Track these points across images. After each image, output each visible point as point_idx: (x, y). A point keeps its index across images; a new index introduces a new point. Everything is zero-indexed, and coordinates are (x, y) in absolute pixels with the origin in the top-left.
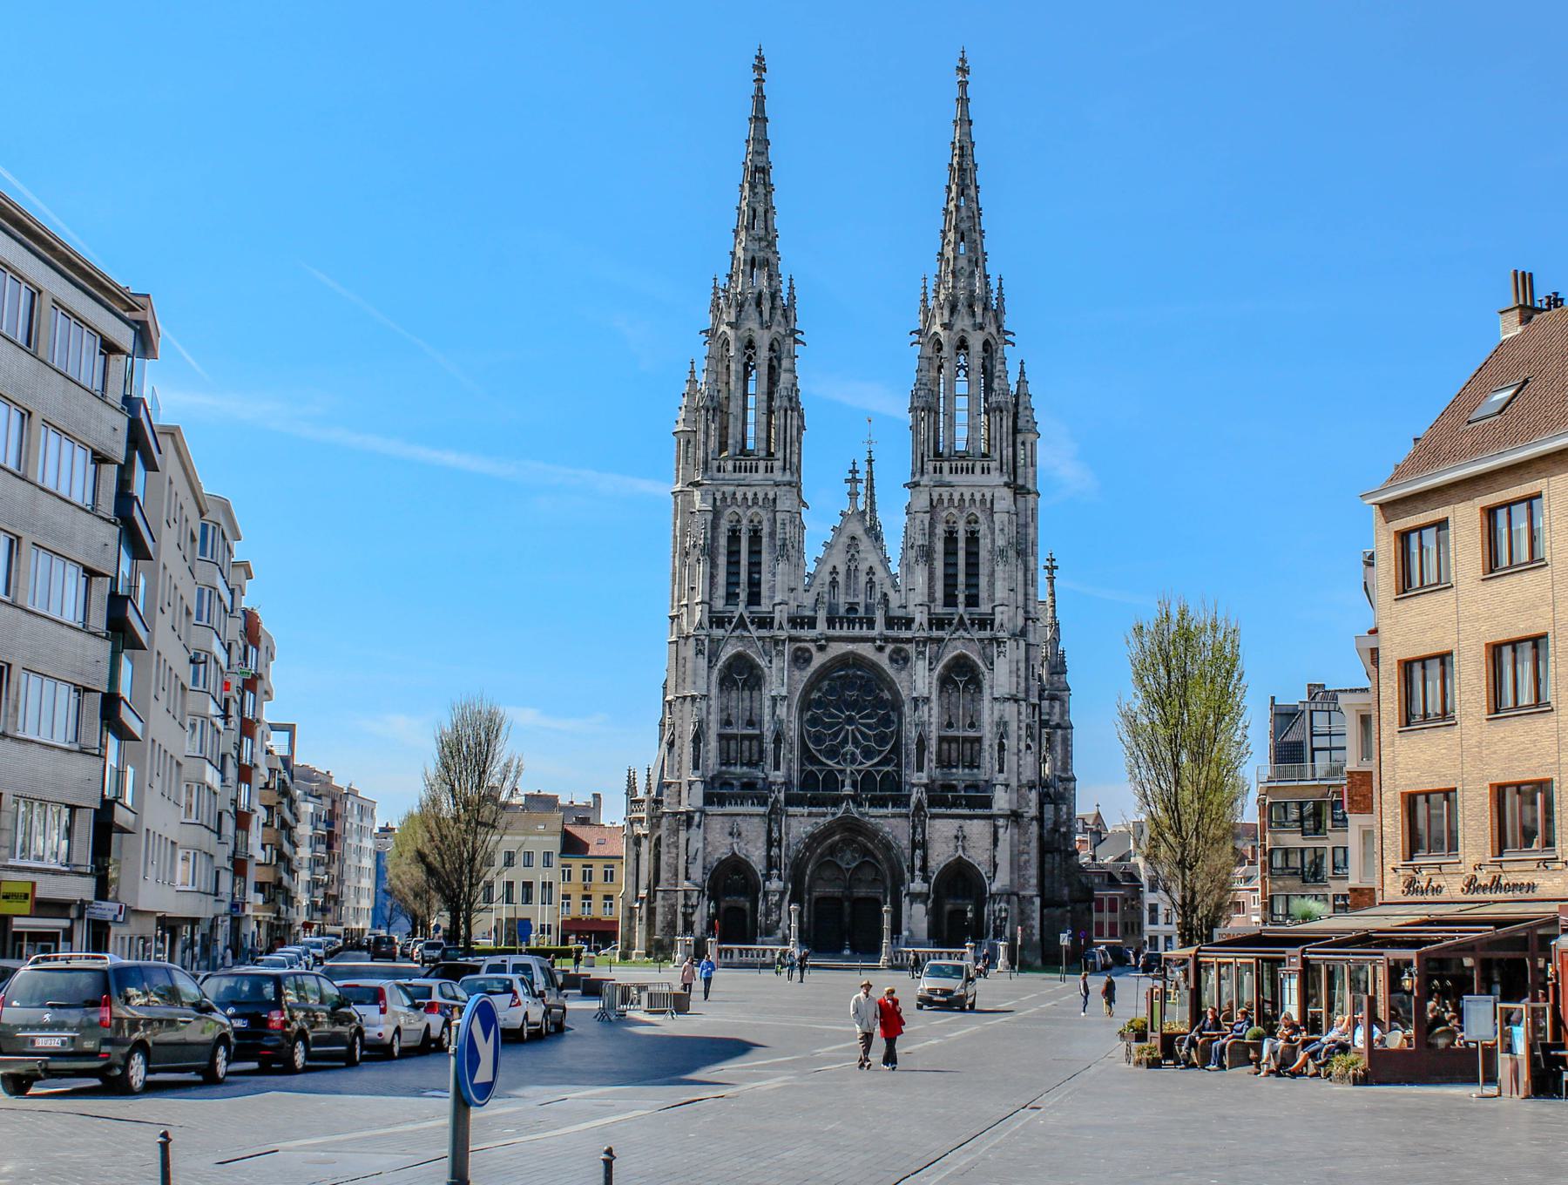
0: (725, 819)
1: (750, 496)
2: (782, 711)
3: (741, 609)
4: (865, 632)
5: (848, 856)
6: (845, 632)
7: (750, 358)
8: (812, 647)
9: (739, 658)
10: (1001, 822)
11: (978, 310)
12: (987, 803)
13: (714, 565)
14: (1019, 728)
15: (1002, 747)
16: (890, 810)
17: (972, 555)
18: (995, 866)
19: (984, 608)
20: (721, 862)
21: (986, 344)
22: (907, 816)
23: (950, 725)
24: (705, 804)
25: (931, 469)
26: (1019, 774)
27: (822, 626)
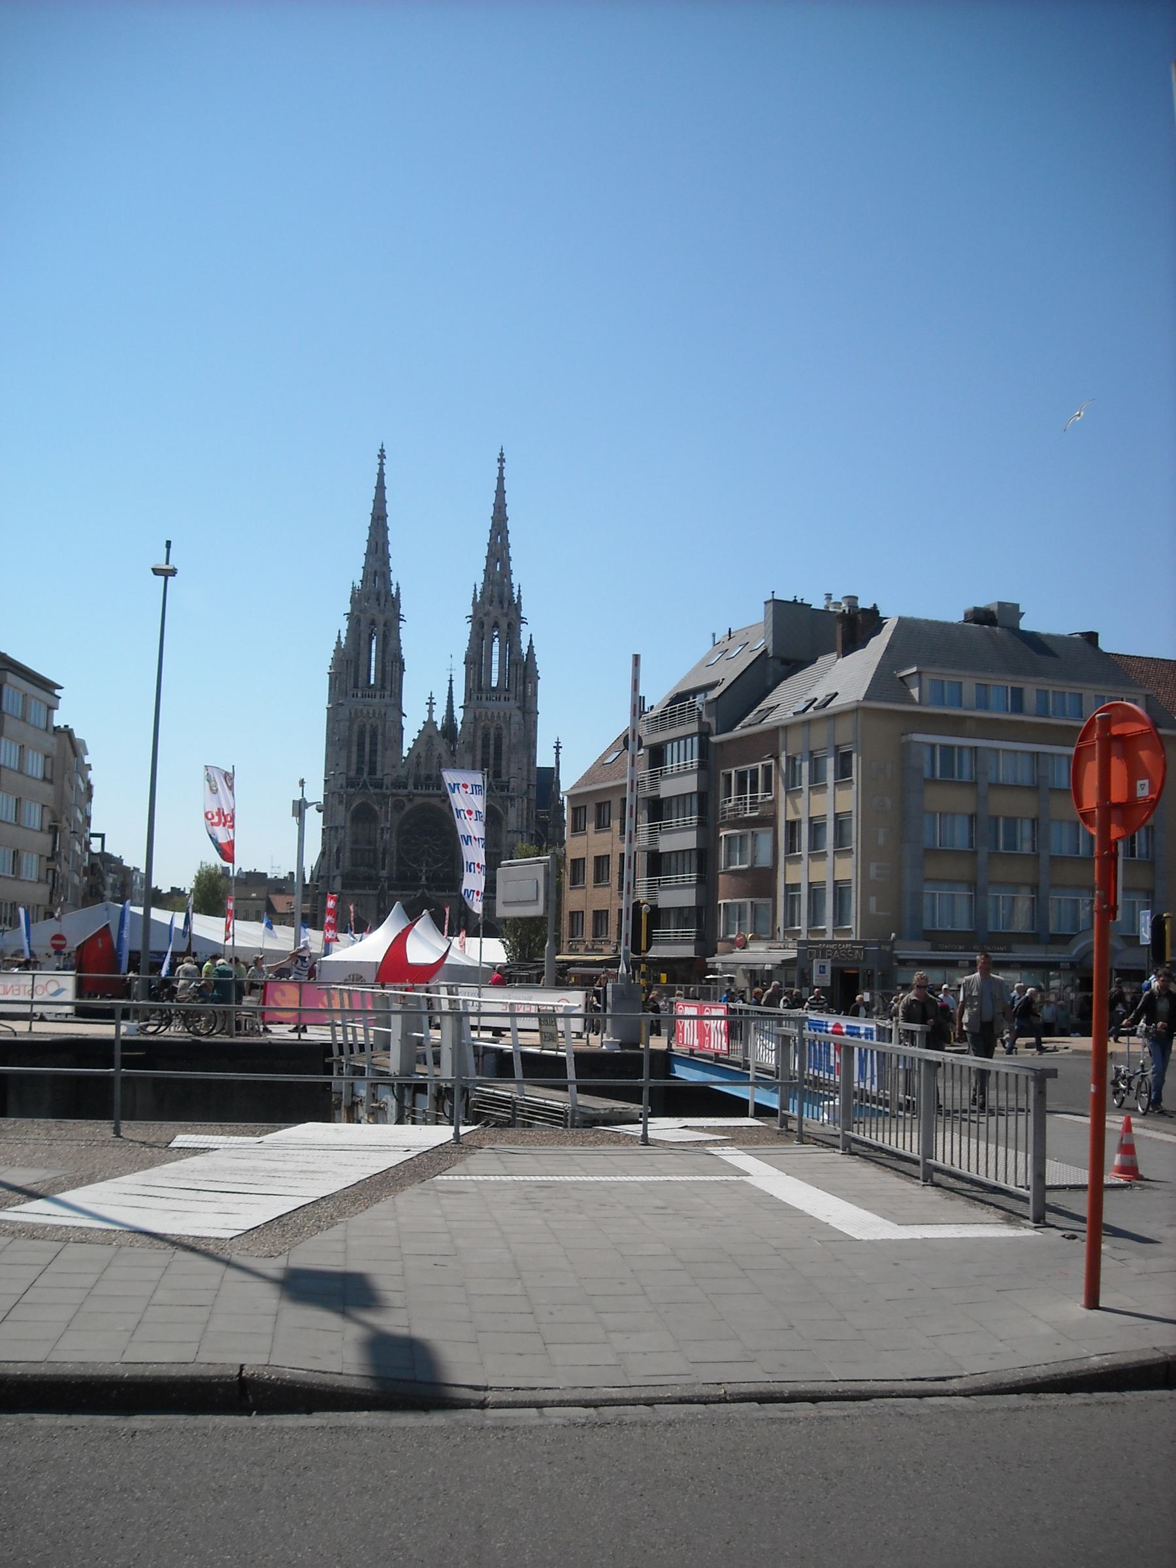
2: (386, 836)
4: (436, 792)
6: (423, 792)
8: (405, 799)
9: (363, 804)
11: (506, 605)
13: (349, 752)
16: (447, 893)
17: (498, 748)
21: (509, 625)
27: (411, 787)
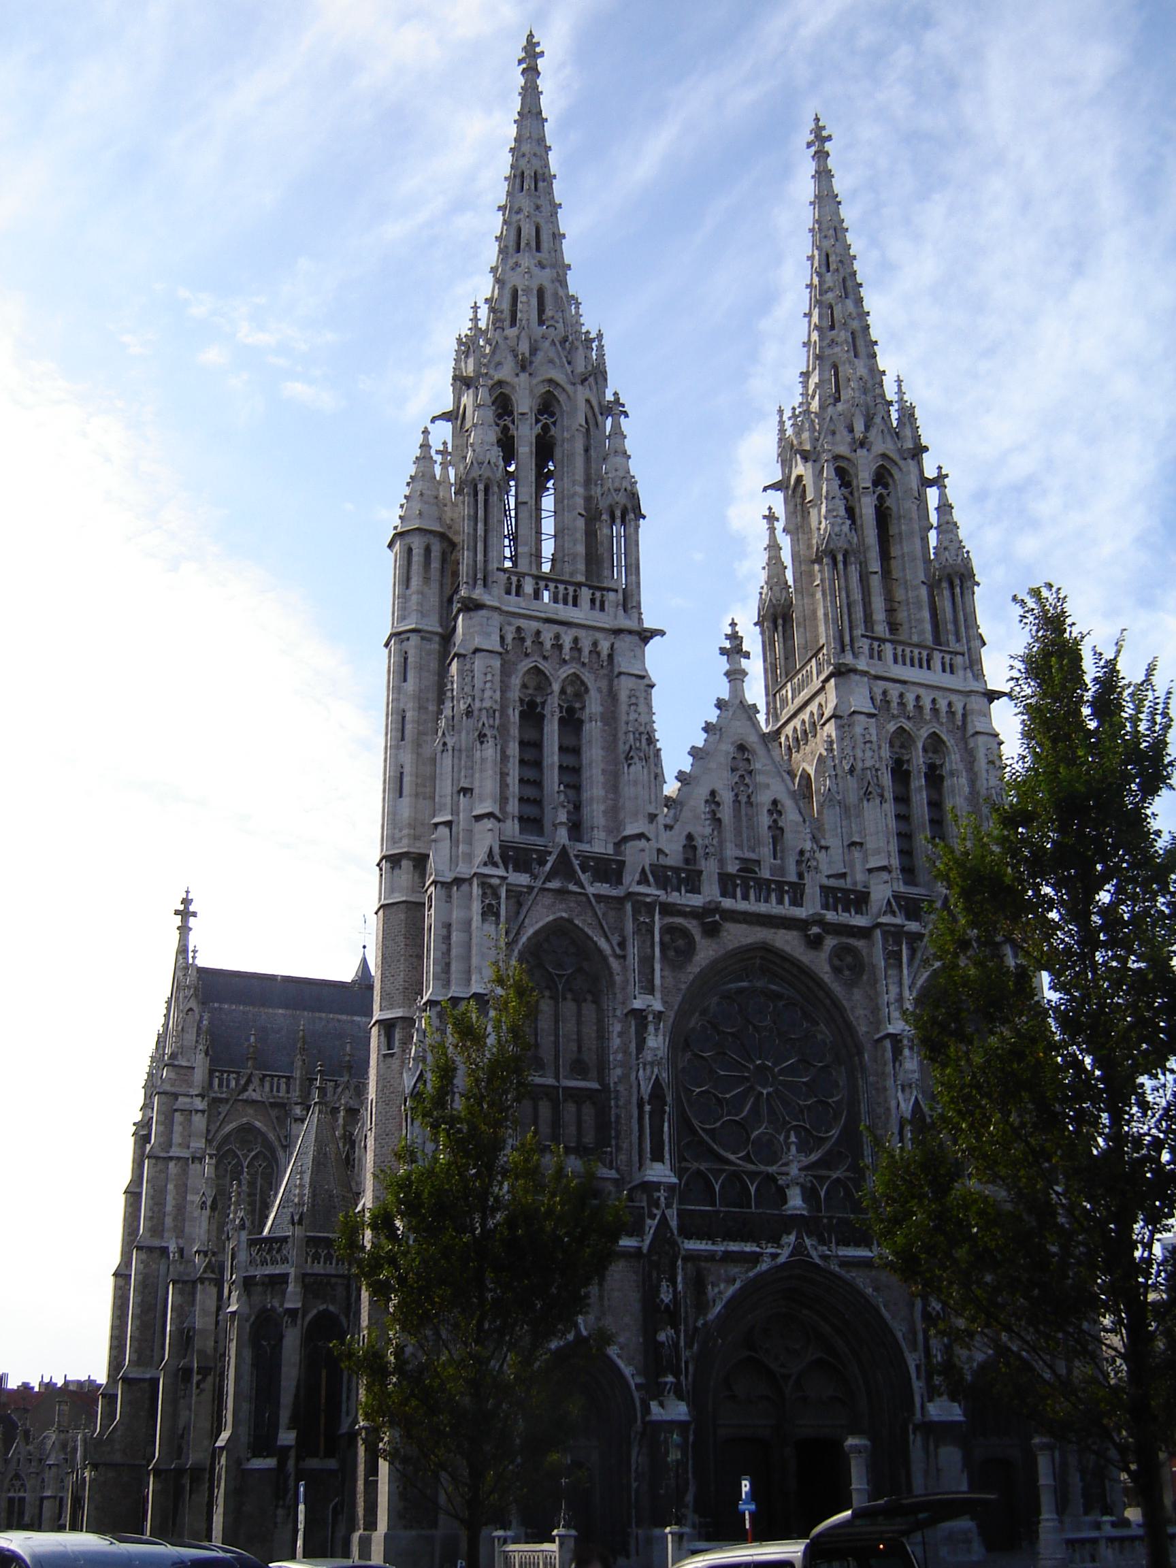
1: (567, 641)
8: (693, 926)
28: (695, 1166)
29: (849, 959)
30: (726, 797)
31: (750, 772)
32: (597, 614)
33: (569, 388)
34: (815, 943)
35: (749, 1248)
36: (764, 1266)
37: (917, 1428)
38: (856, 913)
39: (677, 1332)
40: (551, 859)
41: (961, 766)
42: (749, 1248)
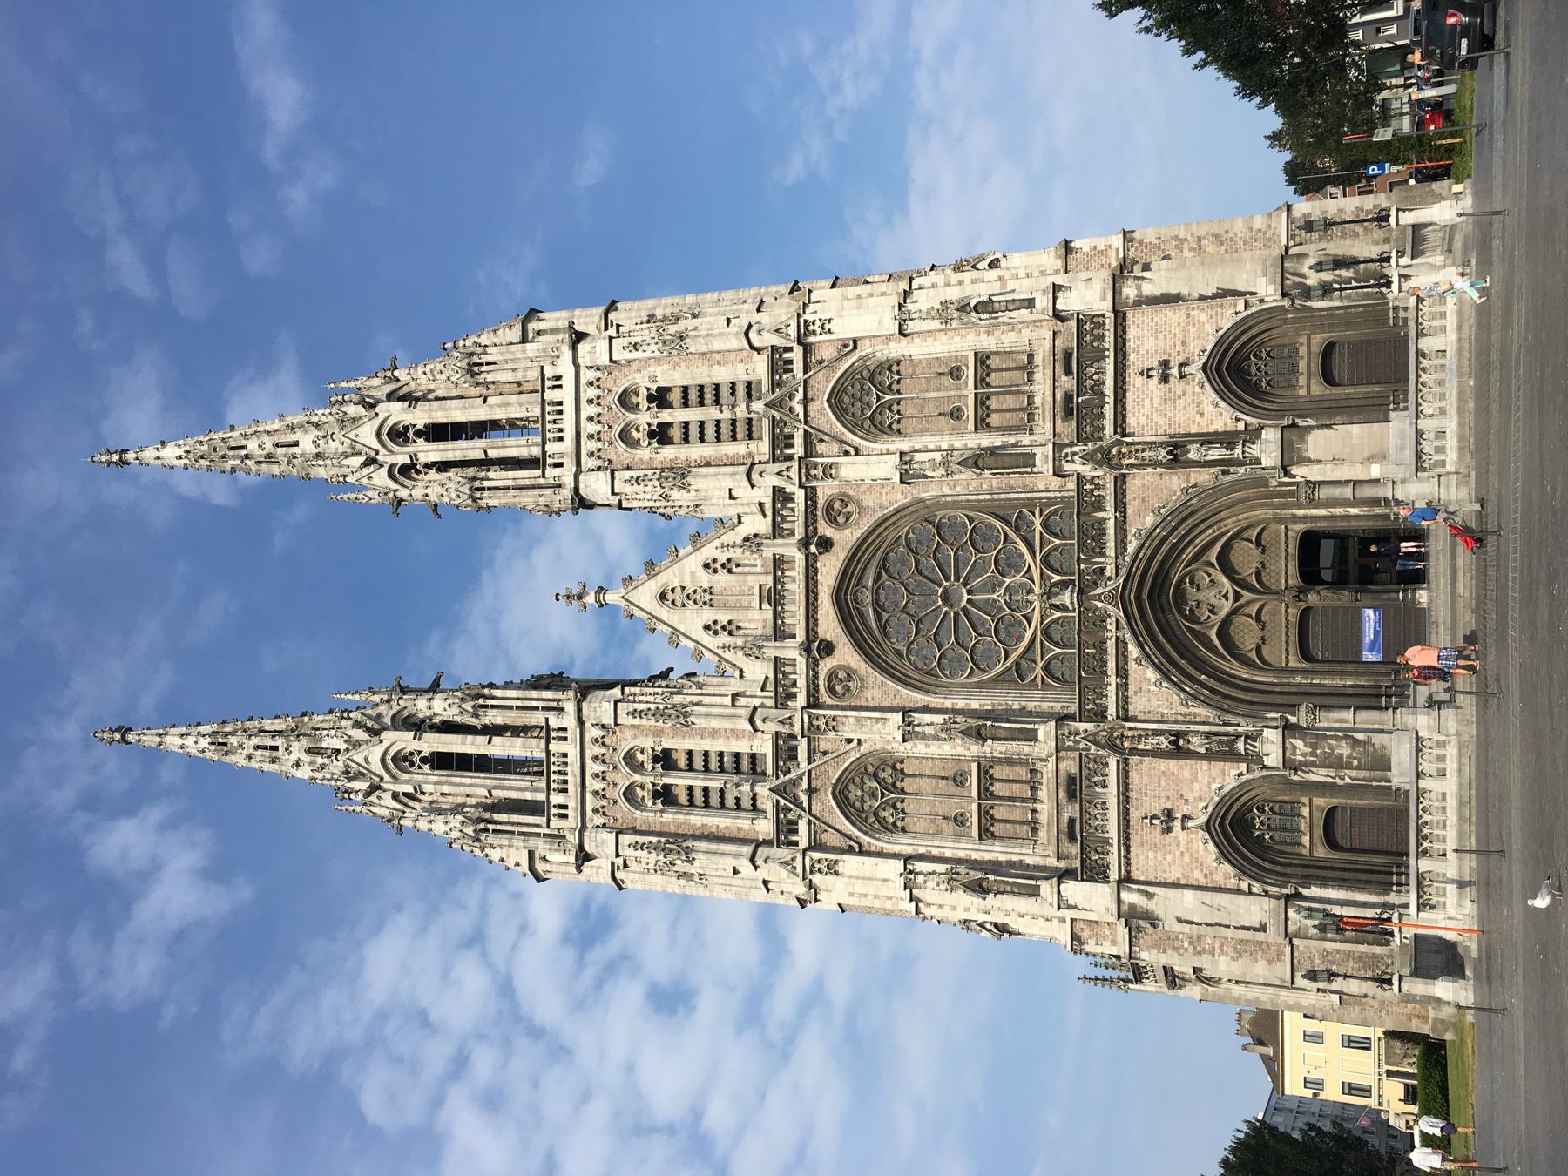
0: (1135, 839)
1: (598, 768)
3: (762, 790)
5: (1211, 596)
7: (424, 760)
10: (1129, 292)
12: (1086, 324)
14: (960, 283)
15: (985, 307)
18: (1223, 294)
19: (760, 368)
20: (1224, 855)
22: (1120, 482)
23: (956, 414)
24: (1105, 879)
25: (557, 472)
26: (1043, 273)
28: (1038, 671)
29: (837, 505)
30: (708, 615)
31: (683, 588)
32: (569, 735)
33: (386, 744)
34: (826, 544)
35: (1111, 644)
36: (1128, 636)
37: (1287, 473)
38: (793, 500)
39: (1197, 732)
40: (783, 802)
41: (646, 373)
42: (1111, 645)
